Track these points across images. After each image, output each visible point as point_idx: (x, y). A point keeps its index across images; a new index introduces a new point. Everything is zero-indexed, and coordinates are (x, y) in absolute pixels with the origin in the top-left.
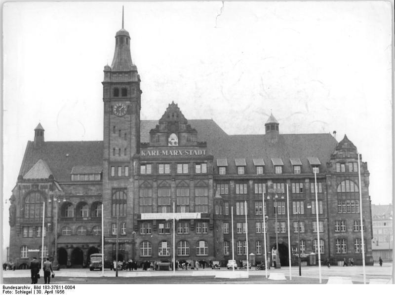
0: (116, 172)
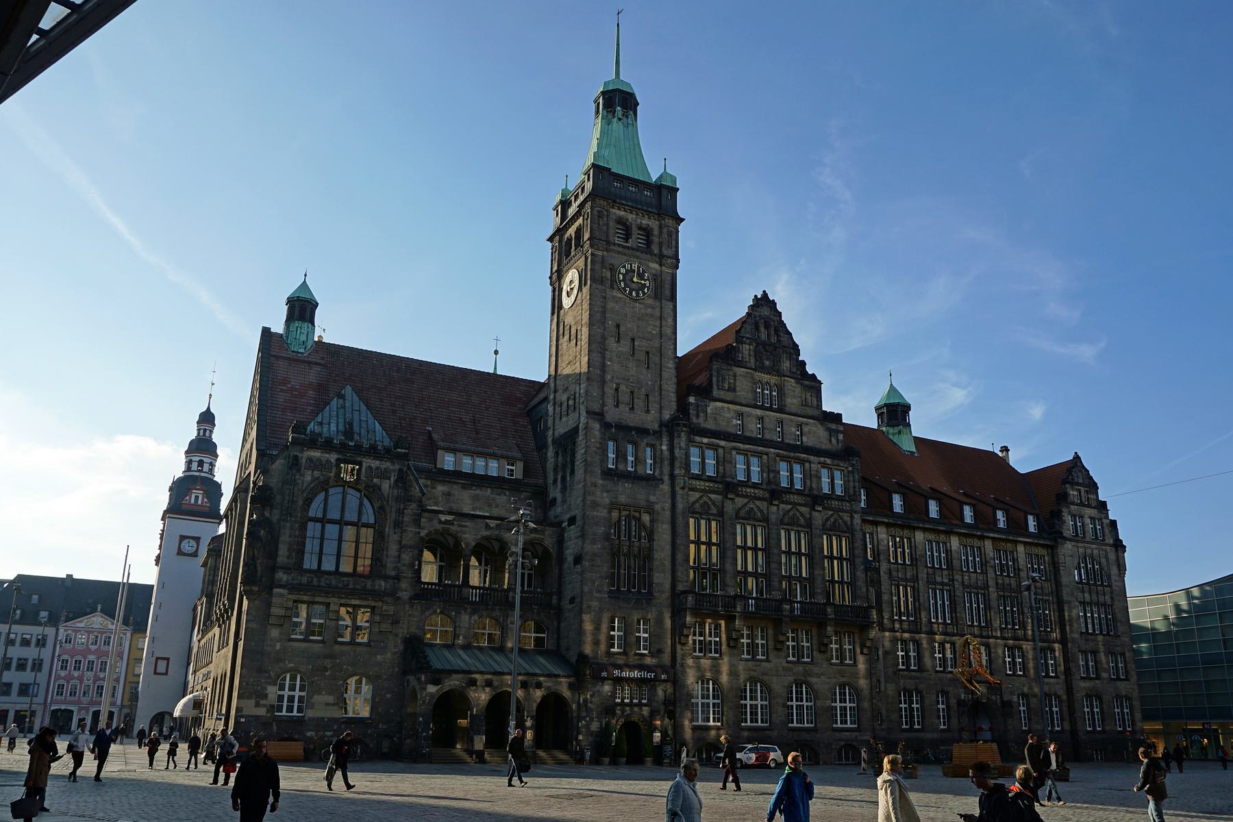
0: (621, 456)
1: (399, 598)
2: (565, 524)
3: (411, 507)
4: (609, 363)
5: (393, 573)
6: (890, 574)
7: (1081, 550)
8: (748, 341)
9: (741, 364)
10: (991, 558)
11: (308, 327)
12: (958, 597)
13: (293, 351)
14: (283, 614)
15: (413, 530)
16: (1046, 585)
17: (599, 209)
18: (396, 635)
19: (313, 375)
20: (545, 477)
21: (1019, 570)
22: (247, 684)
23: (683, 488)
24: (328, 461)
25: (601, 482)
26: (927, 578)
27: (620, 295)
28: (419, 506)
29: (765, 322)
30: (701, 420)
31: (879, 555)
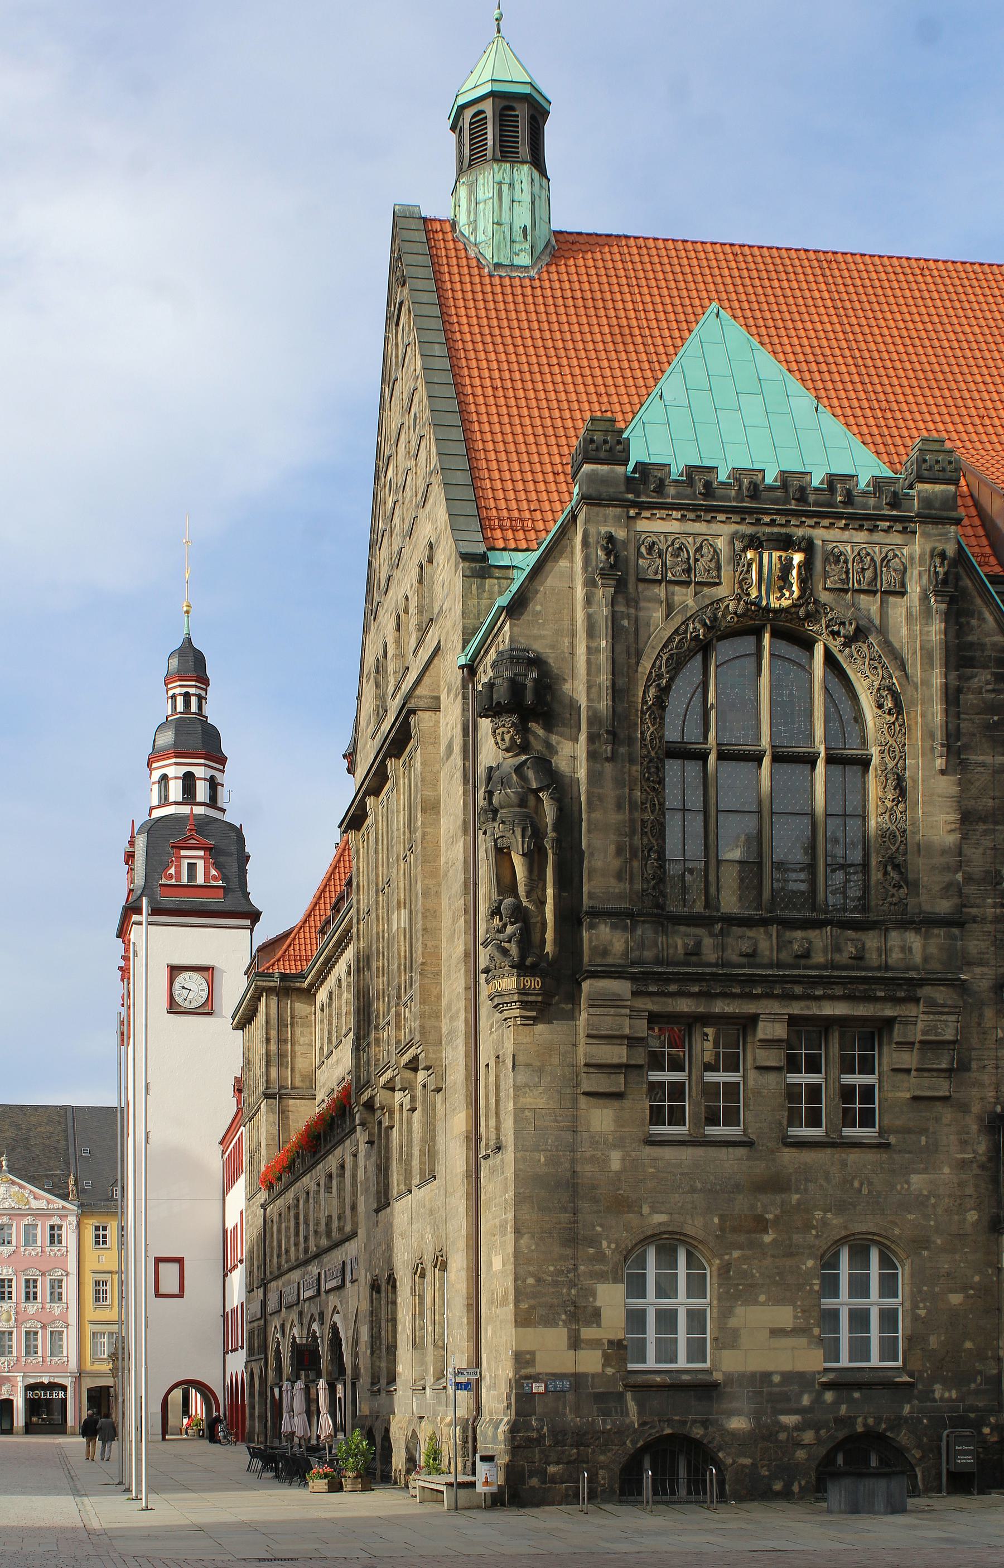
3: (975, 683)
14: (624, 1060)
15: (988, 759)
18: (964, 1108)
22: (539, 1280)
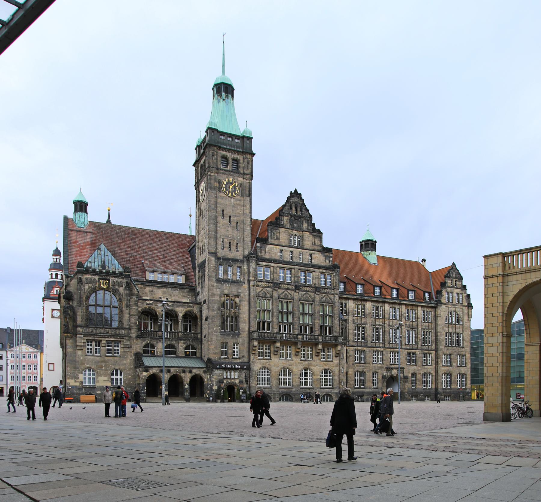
0: (225, 272)
1: (131, 337)
2: (202, 303)
3: (133, 298)
4: (219, 229)
5: (127, 327)
6: (354, 321)
7: (450, 309)
8: (286, 215)
9: (282, 226)
10: (404, 313)
11: (84, 215)
12: (386, 331)
13: (79, 227)
16: (431, 325)
17: (212, 151)
18: (131, 352)
19: (89, 238)
20: (196, 282)
21: (418, 318)
22: (70, 373)
23: (253, 286)
24: (95, 279)
25: (215, 284)
26: (372, 323)
27: (224, 195)
28: (137, 297)
29: (295, 204)
30: (263, 254)
31: (349, 313)
